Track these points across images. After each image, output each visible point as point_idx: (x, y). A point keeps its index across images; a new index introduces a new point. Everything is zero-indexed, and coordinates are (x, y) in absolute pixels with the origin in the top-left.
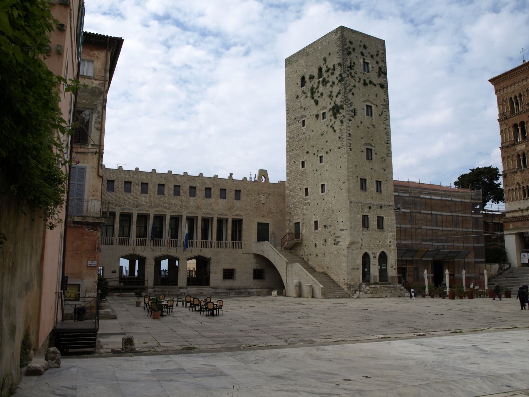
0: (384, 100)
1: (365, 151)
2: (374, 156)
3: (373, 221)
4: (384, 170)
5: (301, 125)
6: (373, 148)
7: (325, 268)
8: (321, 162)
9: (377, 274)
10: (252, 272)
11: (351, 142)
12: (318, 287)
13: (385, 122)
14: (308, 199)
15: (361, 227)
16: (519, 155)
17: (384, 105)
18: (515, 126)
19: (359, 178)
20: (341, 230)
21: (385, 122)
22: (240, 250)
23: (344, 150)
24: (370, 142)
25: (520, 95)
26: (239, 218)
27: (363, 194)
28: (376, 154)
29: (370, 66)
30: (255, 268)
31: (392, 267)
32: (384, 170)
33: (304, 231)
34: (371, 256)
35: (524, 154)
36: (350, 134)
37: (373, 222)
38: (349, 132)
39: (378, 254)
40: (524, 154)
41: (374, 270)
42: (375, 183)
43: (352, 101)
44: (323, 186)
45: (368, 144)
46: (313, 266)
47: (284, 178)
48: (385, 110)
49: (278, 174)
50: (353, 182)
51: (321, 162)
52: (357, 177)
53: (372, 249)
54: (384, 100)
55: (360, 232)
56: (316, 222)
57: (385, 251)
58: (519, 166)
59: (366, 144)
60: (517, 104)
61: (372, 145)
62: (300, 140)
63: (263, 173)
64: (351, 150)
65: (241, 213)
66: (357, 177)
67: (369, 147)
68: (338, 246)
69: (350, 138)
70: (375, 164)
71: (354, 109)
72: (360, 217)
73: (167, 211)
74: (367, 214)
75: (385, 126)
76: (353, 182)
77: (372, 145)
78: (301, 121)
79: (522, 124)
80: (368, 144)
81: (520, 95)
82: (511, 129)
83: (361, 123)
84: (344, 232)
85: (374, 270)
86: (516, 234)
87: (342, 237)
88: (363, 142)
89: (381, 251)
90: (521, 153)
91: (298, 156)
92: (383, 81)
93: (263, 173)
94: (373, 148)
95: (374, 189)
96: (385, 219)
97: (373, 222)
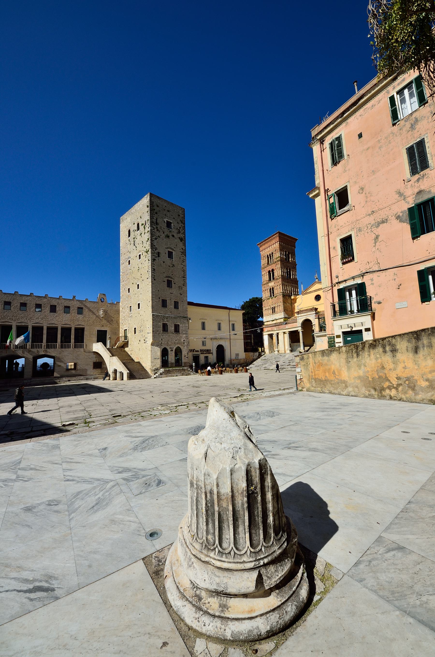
0: (182, 249)
1: (166, 281)
2: (173, 284)
3: (171, 327)
4: (181, 295)
7: (140, 359)
8: (138, 288)
9: (173, 361)
10: (92, 364)
11: (155, 274)
12: (126, 372)
14: (131, 313)
15: (162, 331)
16: (270, 289)
17: (182, 252)
18: (269, 272)
19: (161, 299)
22: (82, 350)
23: (150, 280)
24: (171, 275)
25: (272, 253)
26: (81, 326)
27: (164, 309)
29: (172, 225)
30: (95, 361)
31: (185, 356)
32: (181, 295)
33: (129, 335)
34: (169, 350)
35: (273, 288)
37: (171, 328)
39: (175, 348)
40: (273, 288)
41: (172, 358)
43: (156, 246)
44: (139, 304)
45: (169, 277)
46: (133, 358)
48: (183, 255)
50: (156, 302)
51: (138, 288)
53: (170, 345)
54: (182, 249)
55: (160, 335)
56: (135, 328)
57: (180, 346)
58: (271, 295)
59: (167, 277)
60: (271, 259)
61: (172, 278)
62: (127, 274)
65: (83, 323)
67: (170, 279)
68: (146, 344)
70: (174, 290)
71: (158, 253)
72: (161, 324)
73: (13, 322)
74: (166, 323)
75: (182, 266)
76: (156, 302)
77: (172, 278)
79: (273, 270)
81: (272, 253)
82: (267, 274)
83: (164, 262)
85: (172, 358)
86: (268, 335)
87: (148, 338)
88: (165, 275)
89: (177, 346)
90: (271, 288)
91: (126, 285)
95: (173, 306)
96: (181, 326)
97: (171, 328)
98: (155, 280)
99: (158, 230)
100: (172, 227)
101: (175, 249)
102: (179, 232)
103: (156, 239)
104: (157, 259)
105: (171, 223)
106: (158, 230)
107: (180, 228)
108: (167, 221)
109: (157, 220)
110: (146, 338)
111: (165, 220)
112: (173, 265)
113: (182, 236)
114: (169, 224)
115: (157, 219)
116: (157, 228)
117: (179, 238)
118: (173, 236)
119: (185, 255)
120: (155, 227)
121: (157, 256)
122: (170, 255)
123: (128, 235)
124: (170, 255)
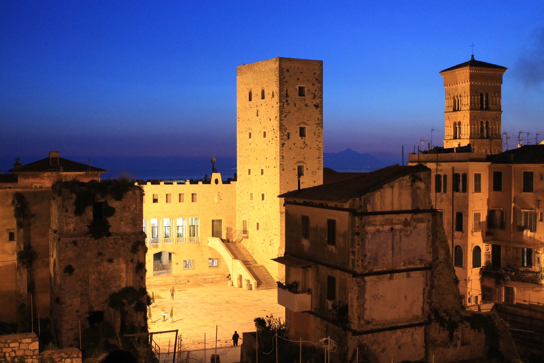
0: (318, 119)
5: (248, 136)
11: (284, 163)
12: (253, 282)
14: (253, 203)
17: (317, 124)
20: (274, 234)
23: (278, 170)
24: (303, 160)
28: (307, 169)
29: (306, 90)
33: (249, 229)
36: (283, 157)
45: (300, 162)
46: (256, 259)
48: (319, 128)
54: (318, 119)
59: (298, 162)
61: (303, 162)
67: (301, 164)
75: (317, 143)
77: (303, 162)
78: (248, 132)
80: (300, 162)
84: (276, 237)
88: (295, 161)
92: (318, 101)
94: (304, 165)
98: (283, 170)
100: (306, 94)
101: (308, 123)
102: (314, 97)
103: (286, 117)
104: (286, 142)
106: (288, 104)
110: (272, 240)
113: (317, 101)
114: (301, 92)
115: (287, 90)
119: (322, 127)
121: (287, 138)
122: (302, 133)
124: (302, 133)
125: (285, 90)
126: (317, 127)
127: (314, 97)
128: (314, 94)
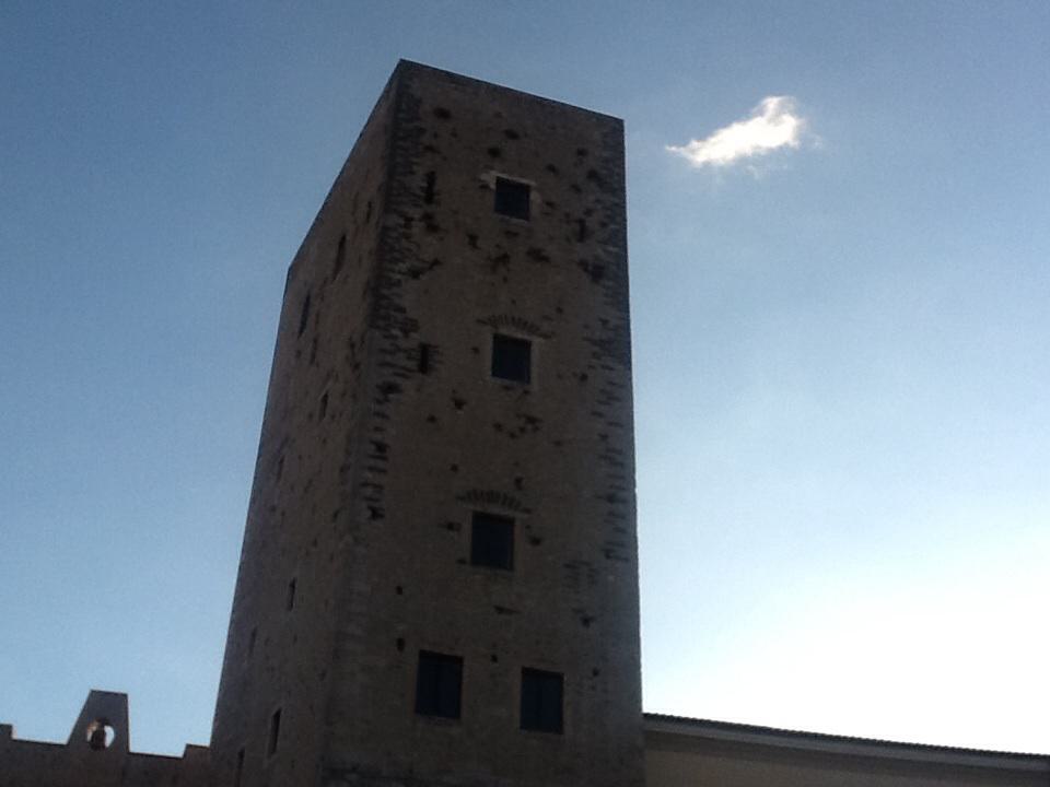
1: (467, 527)
2: (521, 547)
6: (519, 516)
13: (602, 409)
17: (601, 343)
21: (602, 409)
28: (536, 541)
29: (534, 196)
38: (378, 437)
42: (515, 681)
45: (492, 497)
47: (204, 739)
49: (175, 716)
52: (401, 644)
59: (473, 496)
63: (107, 708)
64: (376, 514)
66: (401, 644)
67: (495, 509)
69: (380, 464)
83: (459, 404)
93: (107, 708)
99: (432, 228)
105: (526, 189)
107: (589, 212)
108: (499, 181)
109: (431, 178)
111: (490, 178)
112: (531, 420)
114: (511, 198)
116: (428, 217)
117: (583, 264)
118: (537, 256)
120: (416, 213)
121: (412, 364)
123: (297, 330)
125: (421, 171)
126: (594, 355)
127: (583, 234)
128: (581, 222)
